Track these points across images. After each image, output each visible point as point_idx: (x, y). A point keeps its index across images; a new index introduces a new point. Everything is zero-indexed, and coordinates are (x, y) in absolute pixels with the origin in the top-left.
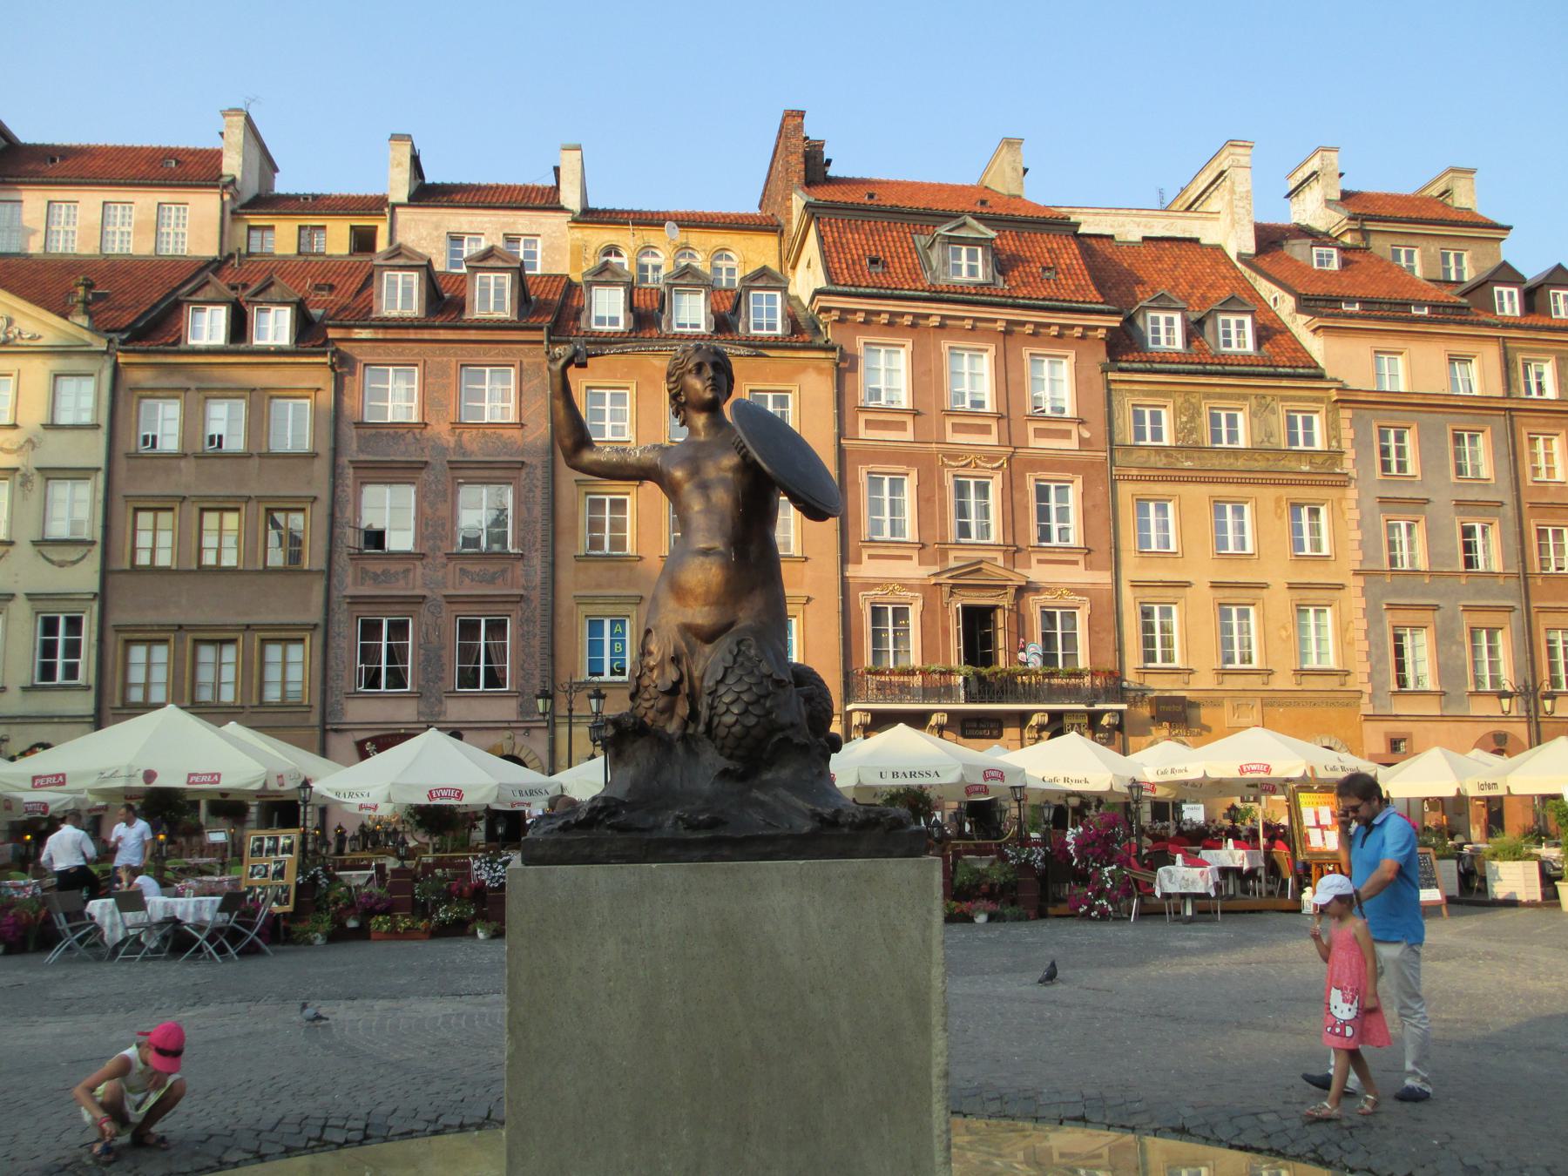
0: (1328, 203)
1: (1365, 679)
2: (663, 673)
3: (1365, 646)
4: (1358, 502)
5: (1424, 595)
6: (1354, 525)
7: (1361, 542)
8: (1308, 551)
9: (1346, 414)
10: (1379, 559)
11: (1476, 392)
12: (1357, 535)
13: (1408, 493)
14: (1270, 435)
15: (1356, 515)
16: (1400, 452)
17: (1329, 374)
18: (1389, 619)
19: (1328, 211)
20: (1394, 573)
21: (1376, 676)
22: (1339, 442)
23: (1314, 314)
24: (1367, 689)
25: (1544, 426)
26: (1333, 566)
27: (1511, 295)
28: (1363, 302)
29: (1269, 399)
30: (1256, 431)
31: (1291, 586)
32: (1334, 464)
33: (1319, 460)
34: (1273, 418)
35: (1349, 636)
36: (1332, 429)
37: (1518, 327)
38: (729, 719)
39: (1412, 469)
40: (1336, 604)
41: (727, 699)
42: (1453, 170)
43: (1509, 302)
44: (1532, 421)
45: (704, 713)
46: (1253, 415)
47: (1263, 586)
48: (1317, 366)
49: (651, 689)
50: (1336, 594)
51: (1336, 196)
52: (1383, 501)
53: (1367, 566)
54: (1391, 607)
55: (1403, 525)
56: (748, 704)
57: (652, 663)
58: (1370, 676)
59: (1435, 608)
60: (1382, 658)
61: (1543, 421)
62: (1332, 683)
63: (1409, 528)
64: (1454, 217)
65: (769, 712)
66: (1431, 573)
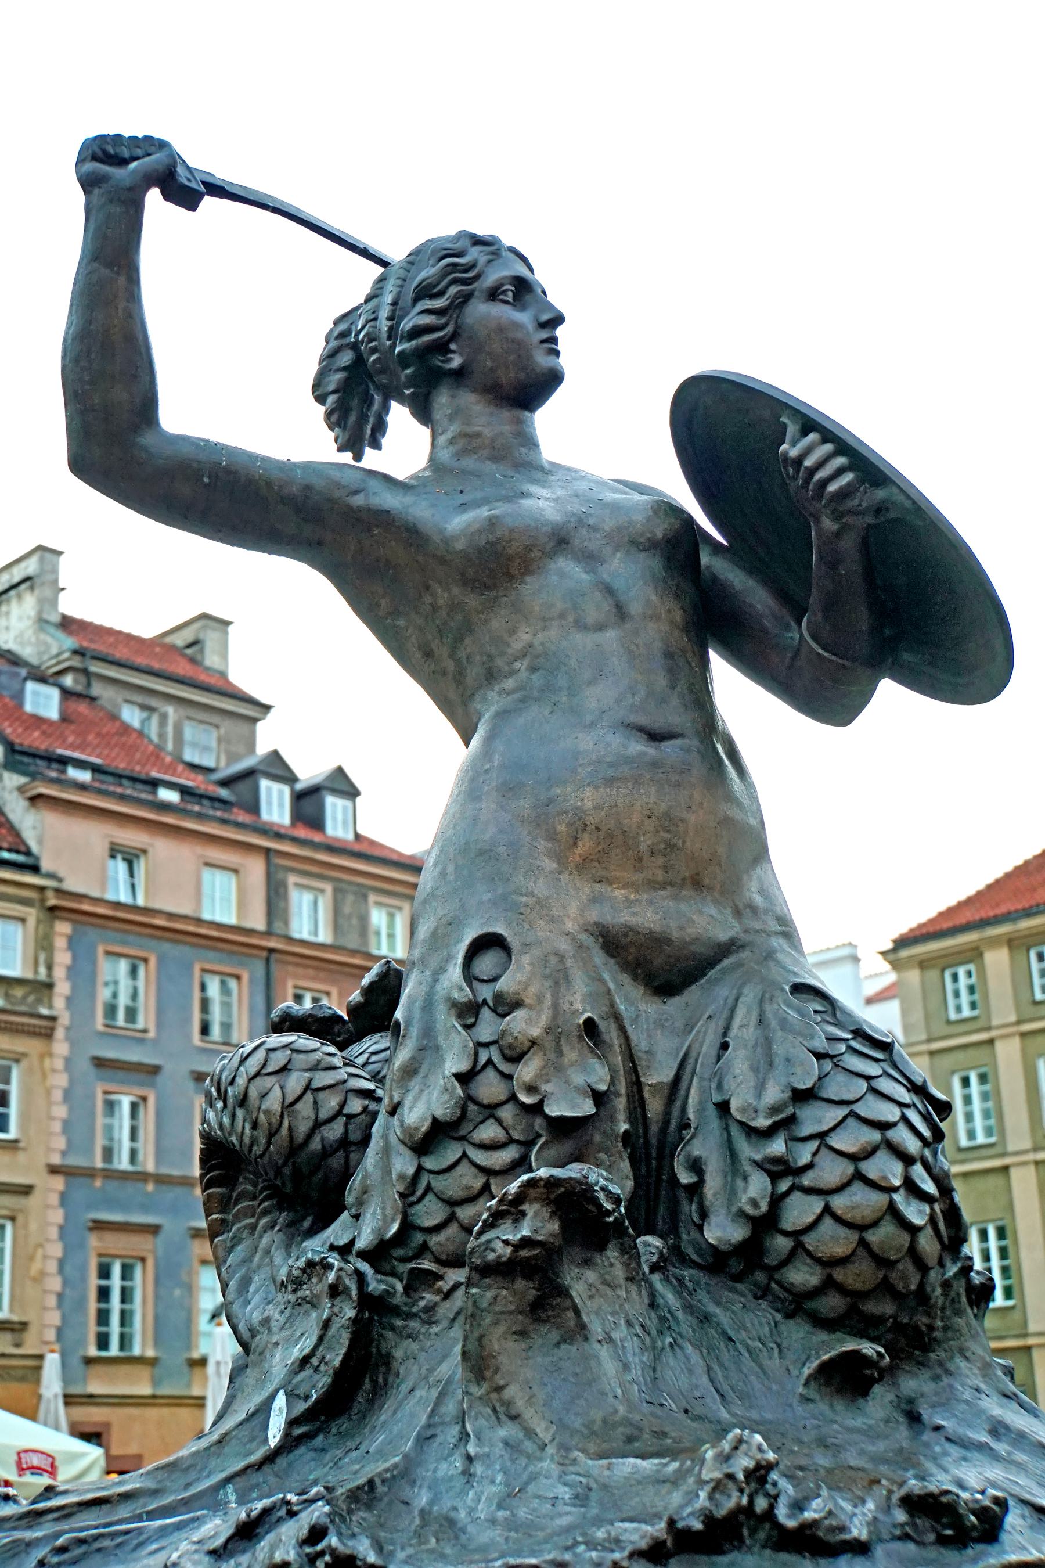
0: (41, 622)
1: (51, 1335)
2: (555, 1068)
3: (55, 1284)
4: (68, 1060)
5: (145, 1209)
6: (58, 1095)
7: (67, 1124)
9: (63, 928)
10: (90, 1151)
12: (61, 1111)
13: (133, 1055)
15: (61, 1080)
17: (45, 865)
18: (94, 1241)
19: (42, 636)
20: (111, 1175)
22: (50, 968)
23: (33, 776)
25: (314, 979)
26: (21, 1157)
27: (281, 793)
28: (95, 769)
32: (39, 1001)
33: (18, 992)
35: (35, 1267)
36: (44, 944)
37: (295, 840)
38: (859, 1201)
40: (20, 1219)
41: (848, 1140)
42: (205, 616)
43: (275, 805)
44: (300, 971)
48: (28, 853)
49: (507, 1113)
51: (55, 618)
52: (100, 1063)
53: (73, 1161)
54: (99, 1226)
55: (126, 1102)
56: (907, 1160)
57: (535, 1032)
58: (60, 1331)
59: (154, 1230)
60: (81, 1304)
61: (311, 972)
63: (134, 1106)
64: (202, 677)
66: (161, 1180)
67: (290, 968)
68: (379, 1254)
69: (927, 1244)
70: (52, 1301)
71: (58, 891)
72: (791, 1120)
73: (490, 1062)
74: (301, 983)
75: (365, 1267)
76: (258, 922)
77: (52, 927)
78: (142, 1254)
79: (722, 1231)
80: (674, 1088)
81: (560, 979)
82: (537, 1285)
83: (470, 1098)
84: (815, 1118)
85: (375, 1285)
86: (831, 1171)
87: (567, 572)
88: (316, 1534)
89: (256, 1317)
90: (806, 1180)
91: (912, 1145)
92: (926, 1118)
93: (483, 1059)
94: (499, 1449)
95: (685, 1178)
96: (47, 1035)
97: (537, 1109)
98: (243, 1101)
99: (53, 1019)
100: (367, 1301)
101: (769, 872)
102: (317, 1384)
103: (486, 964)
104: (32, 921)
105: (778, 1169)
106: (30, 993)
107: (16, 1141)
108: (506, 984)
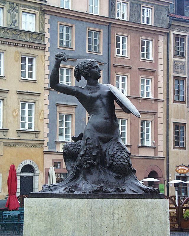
1: (46, 135)
2: (93, 150)
3: (47, 121)
8: (27, 78)
9: (47, 17)
11: (98, 14)
14: (14, 22)
16: (68, 37)
21: (51, 134)
24: (47, 140)
29: (15, 5)
30: (9, 19)
31: (19, 93)
32: (41, 40)
33: (35, 36)
34: (17, 14)
38: (119, 162)
39: (73, 44)
40: (37, 103)
41: (119, 157)
45: (109, 161)
46: (8, 11)
47: (7, 92)
50: (37, 98)
56: (124, 159)
62: (32, 137)
65: (129, 161)
67: (116, 29)
68: (78, 166)
69: (126, 166)
70: (46, 126)
71: (45, 5)
72: (114, 156)
73: (88, 149)
74: (119, 34)
75: (77, 167)
76: (106, 14)
77: (44, 16)
78: (72, 113)
79: (107, 165)
80: (106, 151)
81: (95, 142)
82: (89, 171)
83: (86, 153)
84: (116, 156)
85: (78, 169)
86: (117, 160)
87: (98, 102)
88: (70, 189)
89: (69, 169)
90: (115, 161)
91: (125, 158)
92: (128, 155)
93: (87, 149)
94: (85, 183)
95: (105, 160)
96: (44, 49)
97: (92, 154)
98: (67, 149)
99: (46, 45)
100: (77, 170)
101: (118, 129)
102: (73, 176)
103: (88, 140)
104: (38, 15)
105: (113, 160)
106: (38, 37)
107: (35, 81)
108: (90, 142)
